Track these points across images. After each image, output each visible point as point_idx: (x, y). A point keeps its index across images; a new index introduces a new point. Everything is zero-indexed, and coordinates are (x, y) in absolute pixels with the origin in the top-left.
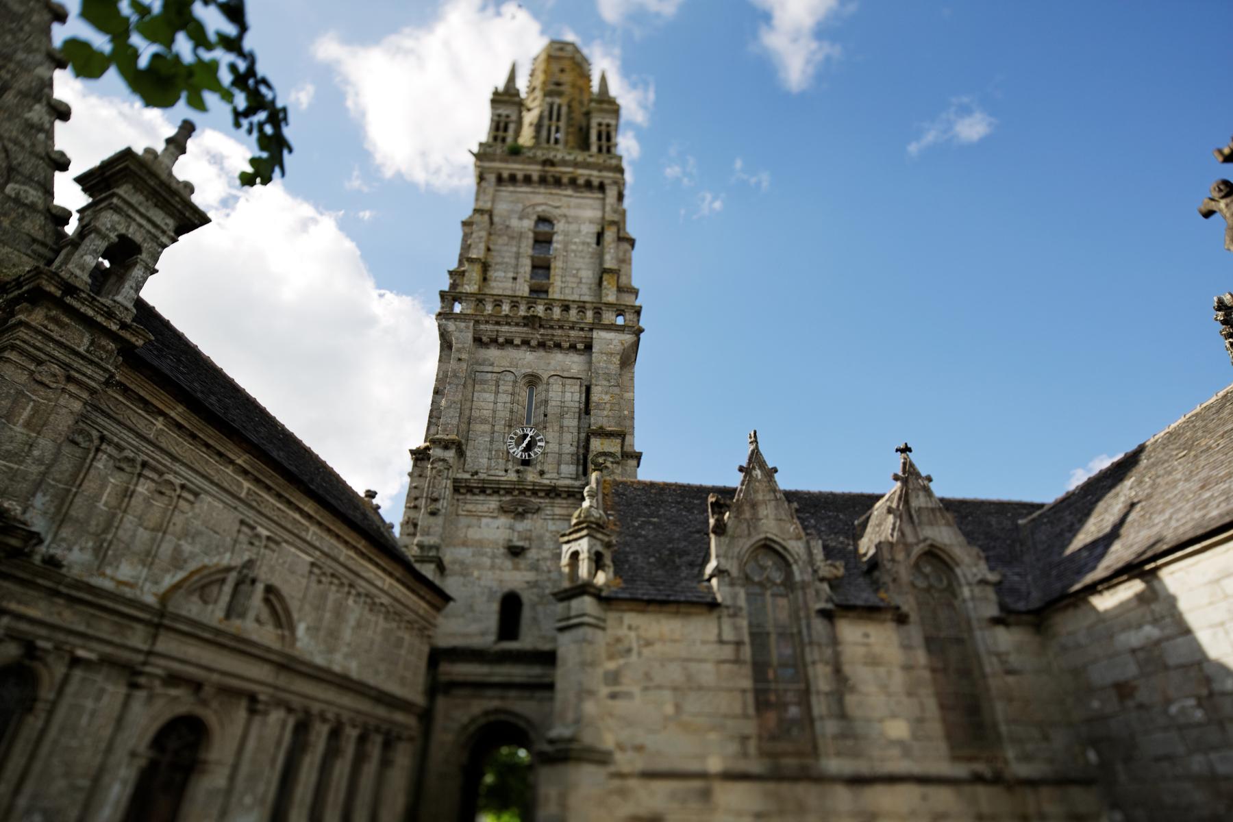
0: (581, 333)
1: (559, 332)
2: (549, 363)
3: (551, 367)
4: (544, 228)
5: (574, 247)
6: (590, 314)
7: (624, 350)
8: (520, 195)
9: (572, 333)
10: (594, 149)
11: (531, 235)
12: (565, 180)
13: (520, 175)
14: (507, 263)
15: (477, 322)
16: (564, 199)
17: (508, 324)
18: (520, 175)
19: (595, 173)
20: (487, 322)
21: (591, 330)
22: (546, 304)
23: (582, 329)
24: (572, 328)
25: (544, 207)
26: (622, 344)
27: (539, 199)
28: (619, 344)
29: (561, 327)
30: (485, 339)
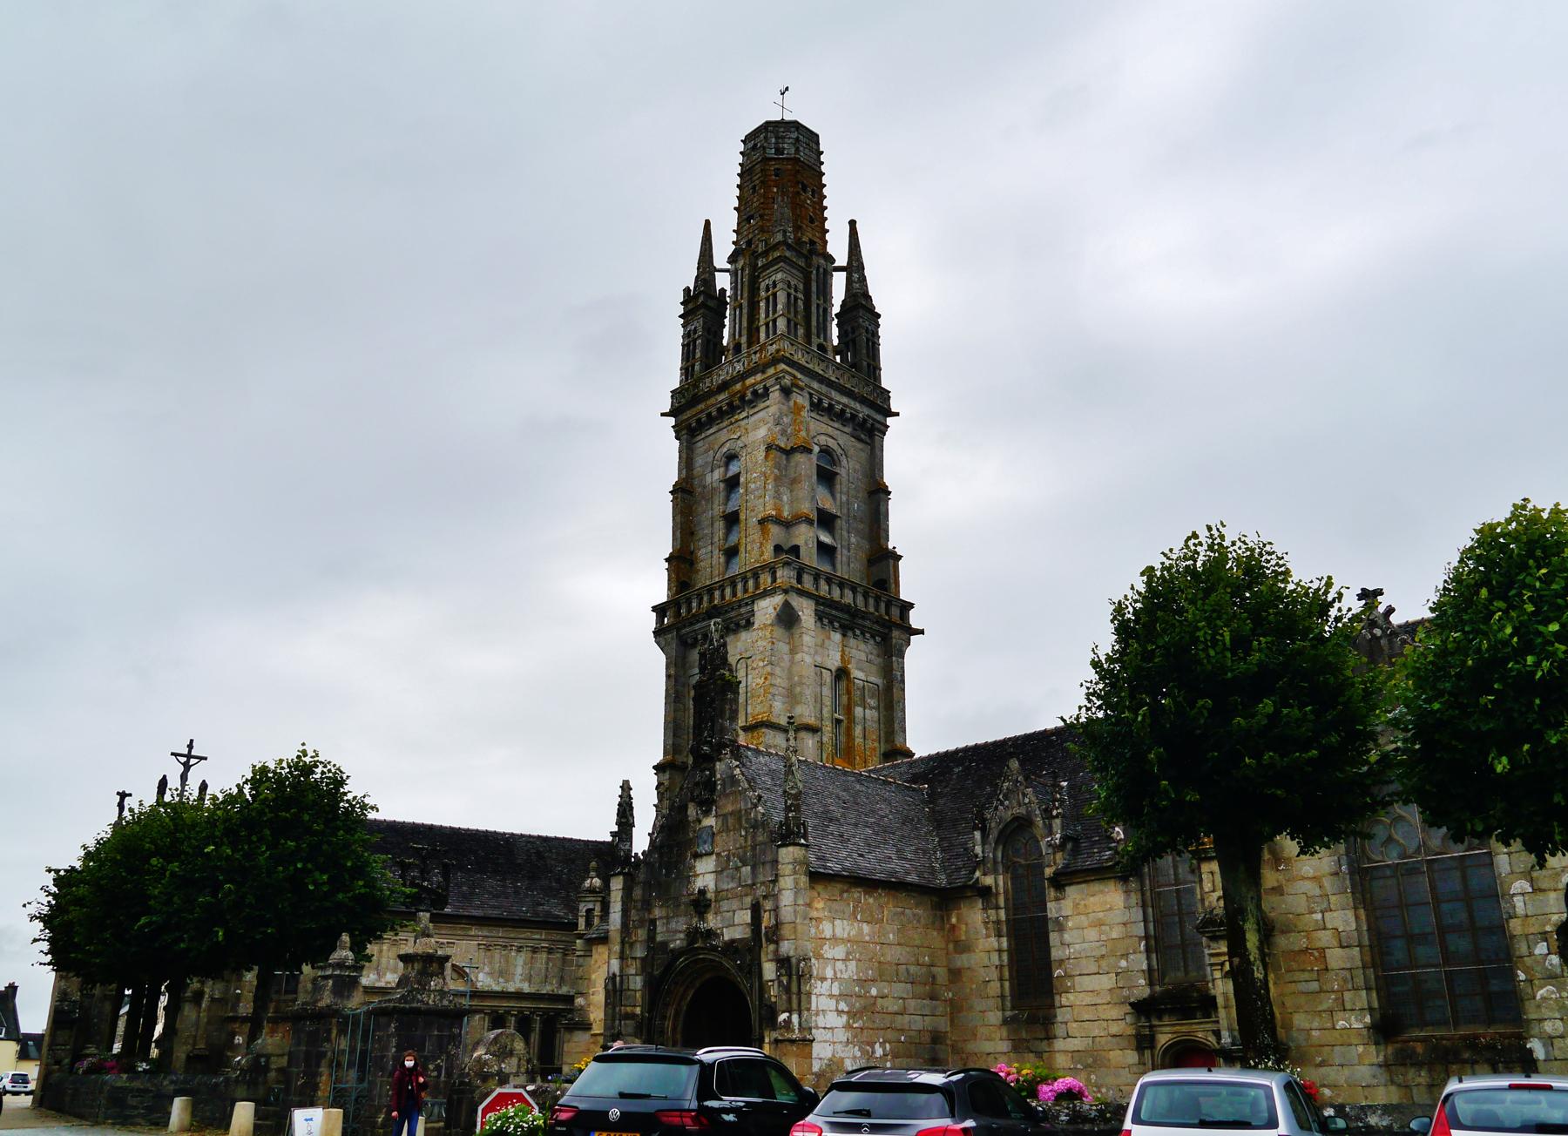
0: (749, 607)
1: (733, 614)
2: (736, 647)
3: (738, 650)
4: (734, 469)
5: (753, 486)
6: (751, 583)
7: (778, 615)
8: (711, 438)
9: (743, 610)
10: (762, 335)
11: (722, 485)
12: (737, 403)
13: (703, 417)
14: (706, 535)
15: (678, 630)
16: (743, 423)
17: (698, 622)
18: (703, 417)
19: (759, 377)
20: (685, 627)
21: (753, 602)
22: (720, 586)
23: (747, 604)
24: (740, 607)
25: (728, 445)
26: (775, 609)
27: (723, 435)
28: (773, 611)
29: (733, 609)
30: (689, 641)
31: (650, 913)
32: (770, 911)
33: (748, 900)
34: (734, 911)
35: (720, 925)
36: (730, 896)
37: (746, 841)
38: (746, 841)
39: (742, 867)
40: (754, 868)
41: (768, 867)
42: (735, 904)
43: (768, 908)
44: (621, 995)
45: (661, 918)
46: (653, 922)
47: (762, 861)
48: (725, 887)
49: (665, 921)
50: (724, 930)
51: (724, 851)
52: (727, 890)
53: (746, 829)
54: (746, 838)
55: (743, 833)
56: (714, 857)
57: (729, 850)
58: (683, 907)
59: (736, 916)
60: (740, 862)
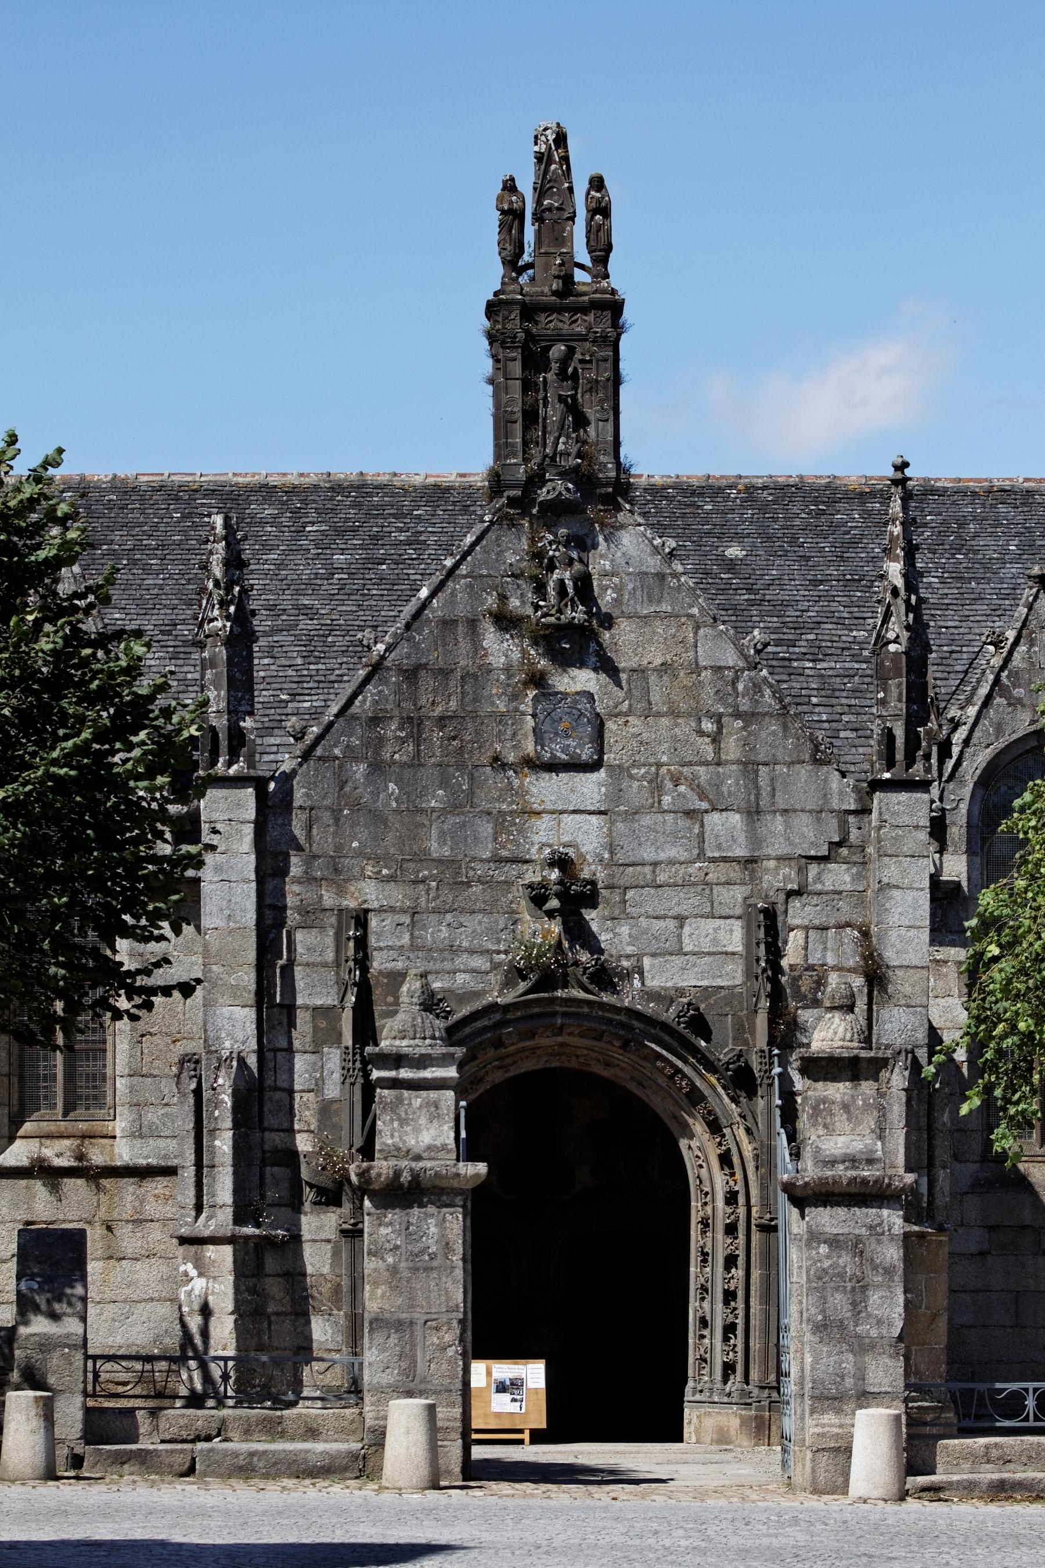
31: (341, 892)
32: (806, 929)
33: (734, 897)
34: (681, 920)
35: (629, 950)
36: (662, 878)
37: (718, 751)
38: (718, 751)
39: (706, 811)
40: (753, 813)
41: (804, 823)
42: (687, 902)
43: (797, 921)
44: (261, 1106)
45: (392, 909)
46: (361, 919)
47: (782, 806)
48: (648, 854)
49: (406, 919)
50: (647, 962)
51: (635, 764)
52: (655, 864)
53: (718, 719)
54: (716, 739)
55: (708, 726)
56: (602, 774)
57: (659, 765)
58: (477, 889)
59: (687, 930)
60: (702, 796)
